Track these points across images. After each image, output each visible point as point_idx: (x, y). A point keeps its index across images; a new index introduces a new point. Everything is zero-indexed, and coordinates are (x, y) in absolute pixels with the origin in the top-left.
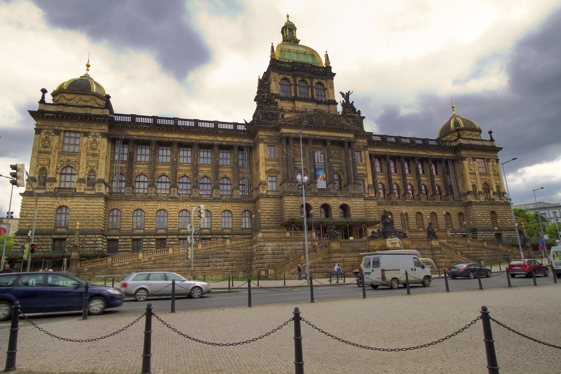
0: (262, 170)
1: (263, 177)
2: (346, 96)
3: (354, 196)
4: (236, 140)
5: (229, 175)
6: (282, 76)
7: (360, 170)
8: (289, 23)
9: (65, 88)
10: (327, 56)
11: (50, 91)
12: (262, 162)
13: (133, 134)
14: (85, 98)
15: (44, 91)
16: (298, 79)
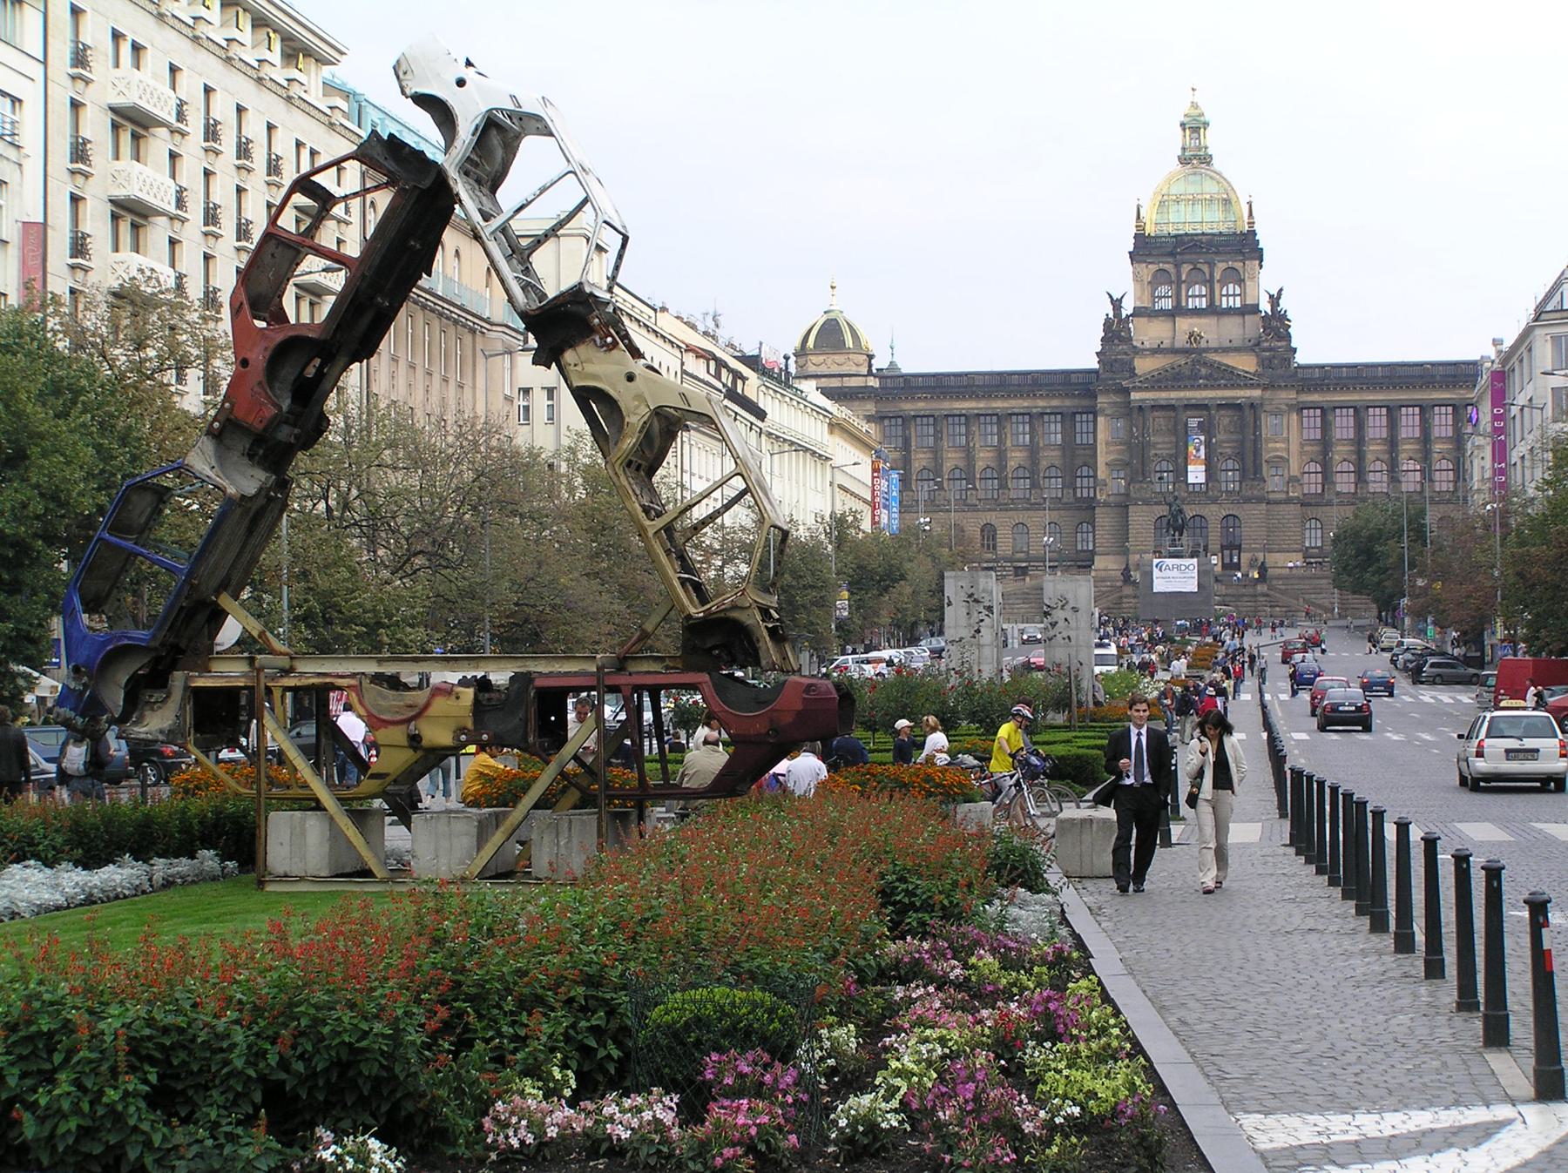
0: (1101, 460)
1: (1102, 473)
2: (1275, 300)
3: (1247, 500)
4: (1068, 403)
5: (1057, 463)
6: (1153, 268)
7: (1277, 450)
8: (1194, 112)
9: (811, 343)
10: (1250, 204)
11: (790, 353)
12: (1101, 448)
13: (908, 407)
14: (839, 358)
15: (787, 358)
16: (1186, 268)
